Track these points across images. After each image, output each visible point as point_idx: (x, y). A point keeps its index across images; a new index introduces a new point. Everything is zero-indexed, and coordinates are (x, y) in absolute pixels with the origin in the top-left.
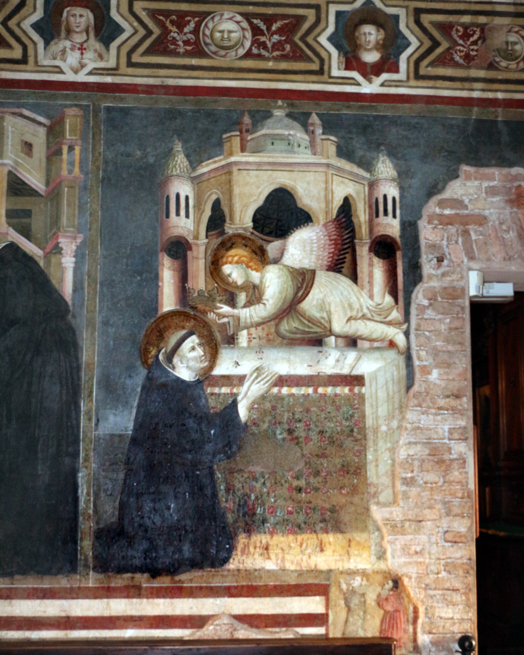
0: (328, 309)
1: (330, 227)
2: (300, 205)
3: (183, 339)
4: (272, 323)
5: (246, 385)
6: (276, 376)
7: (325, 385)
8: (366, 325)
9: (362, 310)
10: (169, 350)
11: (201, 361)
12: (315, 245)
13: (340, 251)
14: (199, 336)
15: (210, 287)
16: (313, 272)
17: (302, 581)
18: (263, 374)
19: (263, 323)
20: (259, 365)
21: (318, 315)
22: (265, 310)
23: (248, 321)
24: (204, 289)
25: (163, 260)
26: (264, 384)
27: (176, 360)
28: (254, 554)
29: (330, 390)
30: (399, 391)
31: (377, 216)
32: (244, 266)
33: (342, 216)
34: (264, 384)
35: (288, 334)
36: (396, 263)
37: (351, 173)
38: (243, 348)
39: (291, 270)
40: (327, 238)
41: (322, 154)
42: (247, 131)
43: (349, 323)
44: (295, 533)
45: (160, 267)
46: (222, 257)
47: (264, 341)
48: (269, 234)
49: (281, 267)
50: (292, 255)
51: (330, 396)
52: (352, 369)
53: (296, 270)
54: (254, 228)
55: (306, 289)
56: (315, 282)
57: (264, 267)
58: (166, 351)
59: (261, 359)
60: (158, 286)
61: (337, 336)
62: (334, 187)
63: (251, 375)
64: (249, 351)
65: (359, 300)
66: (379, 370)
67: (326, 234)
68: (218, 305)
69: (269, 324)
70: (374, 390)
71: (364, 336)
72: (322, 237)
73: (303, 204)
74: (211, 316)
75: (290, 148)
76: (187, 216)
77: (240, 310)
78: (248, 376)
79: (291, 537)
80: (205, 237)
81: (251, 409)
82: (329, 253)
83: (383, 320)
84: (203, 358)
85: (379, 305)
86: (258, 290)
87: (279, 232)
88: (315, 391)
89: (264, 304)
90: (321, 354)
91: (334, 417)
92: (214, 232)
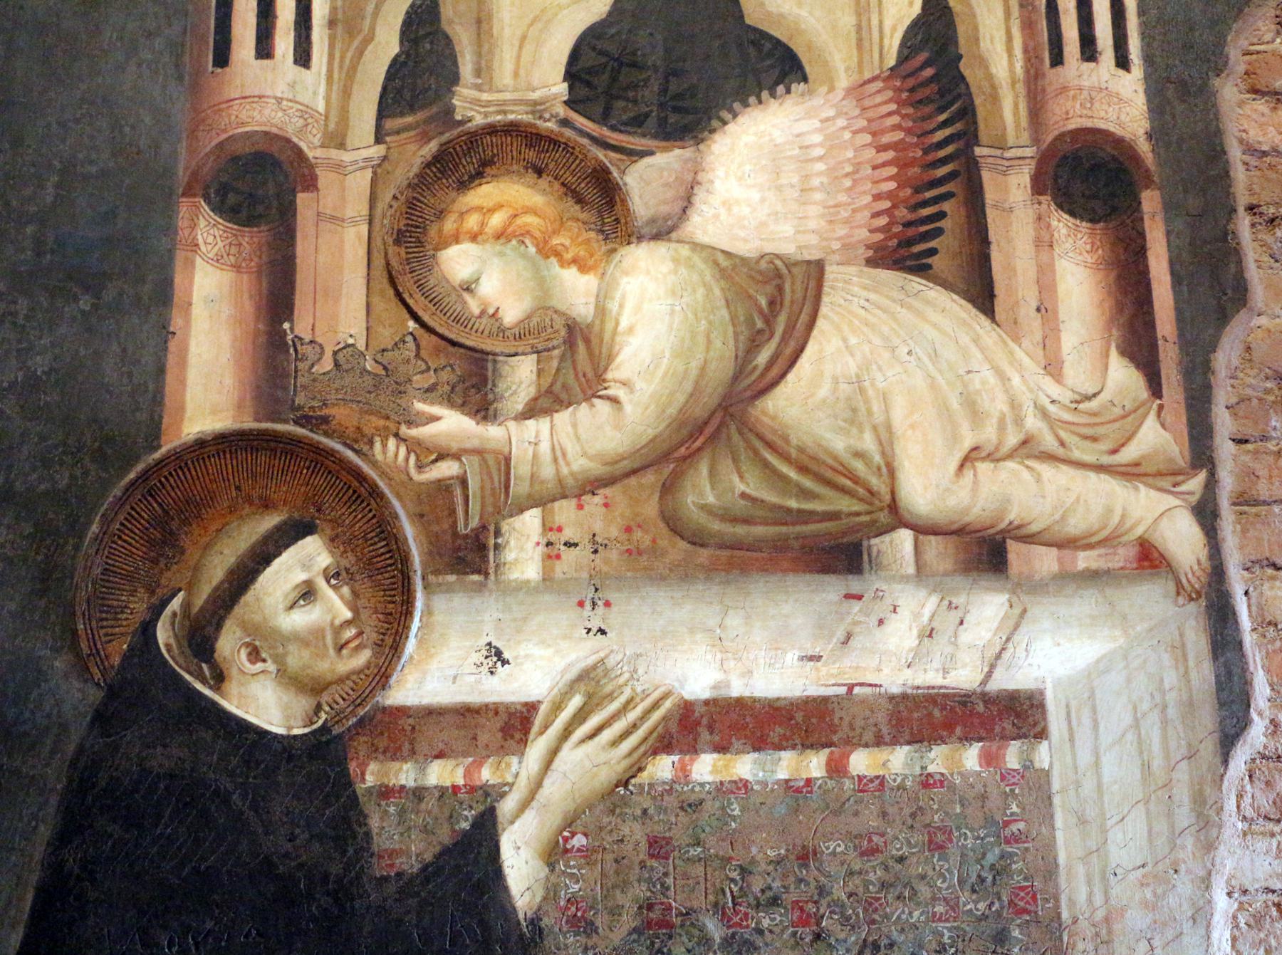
0: (879, 417)
1: (879, 99)
3: (262, 556)
4: (650, 478)
5: (537, 749)
6: (668, 704)
7: (879, 742)
8: (1038, 479)
9: (1019, 421)
10: (199, 602)
11: (340, 648)
12: (820, 167)
13: (917, 191)
15: (386, 336)
16: (817, 270)
18: (610, 697)
19: (609, 481)
20: (591, 661)
21: (839, 444)
22: (617, 427)
23: (547, 472)
24: (361, 345)
25: (193, 226)
26: (615, 743)
27: (229, 643)
31: (1057, 59)
32: (532, 250)
33: (923, 56)
34: (615, 743)
35: (716, 526)
36: (1142, 235)
38: (522, 587)
39: (724, 262)
40: (868, 138)
43: (968, 473)
45: (180, 256)
46: (441, 214)
47: (614, 555)
48: (636, 123)
49: (685, 251)
50: (727, 204)
52: (992, 667)
53: (744, 261)
55: (784, 340)
56: (824, 310)
57: (614, 251)
58: (186, 605)
59: (602, 631)
60: (164, 332)
61: (923, 530)
63: (557, 707)
64: (548, 598)
65: (1003, 378)
66: (1100, 668)
68: (420, 406)
69: (633, 481)
70: (1085, 757)
71: (1034, 528)
72: (847, 135)
73: (769, 14)
74: (390, 452)
76: (303, 57)
77: (512, 425)
78: (543, 709)
81: (554, 853)
82: (877, 197)
83: (1106, 460)
84: (350, 633)
85: (1089, 398)
86: (587, 341)
87: (673, 119)
88: (837, 768)
89: (614, 400)
90: (856, 606)
91: (923, 877)
92: (409, 119)
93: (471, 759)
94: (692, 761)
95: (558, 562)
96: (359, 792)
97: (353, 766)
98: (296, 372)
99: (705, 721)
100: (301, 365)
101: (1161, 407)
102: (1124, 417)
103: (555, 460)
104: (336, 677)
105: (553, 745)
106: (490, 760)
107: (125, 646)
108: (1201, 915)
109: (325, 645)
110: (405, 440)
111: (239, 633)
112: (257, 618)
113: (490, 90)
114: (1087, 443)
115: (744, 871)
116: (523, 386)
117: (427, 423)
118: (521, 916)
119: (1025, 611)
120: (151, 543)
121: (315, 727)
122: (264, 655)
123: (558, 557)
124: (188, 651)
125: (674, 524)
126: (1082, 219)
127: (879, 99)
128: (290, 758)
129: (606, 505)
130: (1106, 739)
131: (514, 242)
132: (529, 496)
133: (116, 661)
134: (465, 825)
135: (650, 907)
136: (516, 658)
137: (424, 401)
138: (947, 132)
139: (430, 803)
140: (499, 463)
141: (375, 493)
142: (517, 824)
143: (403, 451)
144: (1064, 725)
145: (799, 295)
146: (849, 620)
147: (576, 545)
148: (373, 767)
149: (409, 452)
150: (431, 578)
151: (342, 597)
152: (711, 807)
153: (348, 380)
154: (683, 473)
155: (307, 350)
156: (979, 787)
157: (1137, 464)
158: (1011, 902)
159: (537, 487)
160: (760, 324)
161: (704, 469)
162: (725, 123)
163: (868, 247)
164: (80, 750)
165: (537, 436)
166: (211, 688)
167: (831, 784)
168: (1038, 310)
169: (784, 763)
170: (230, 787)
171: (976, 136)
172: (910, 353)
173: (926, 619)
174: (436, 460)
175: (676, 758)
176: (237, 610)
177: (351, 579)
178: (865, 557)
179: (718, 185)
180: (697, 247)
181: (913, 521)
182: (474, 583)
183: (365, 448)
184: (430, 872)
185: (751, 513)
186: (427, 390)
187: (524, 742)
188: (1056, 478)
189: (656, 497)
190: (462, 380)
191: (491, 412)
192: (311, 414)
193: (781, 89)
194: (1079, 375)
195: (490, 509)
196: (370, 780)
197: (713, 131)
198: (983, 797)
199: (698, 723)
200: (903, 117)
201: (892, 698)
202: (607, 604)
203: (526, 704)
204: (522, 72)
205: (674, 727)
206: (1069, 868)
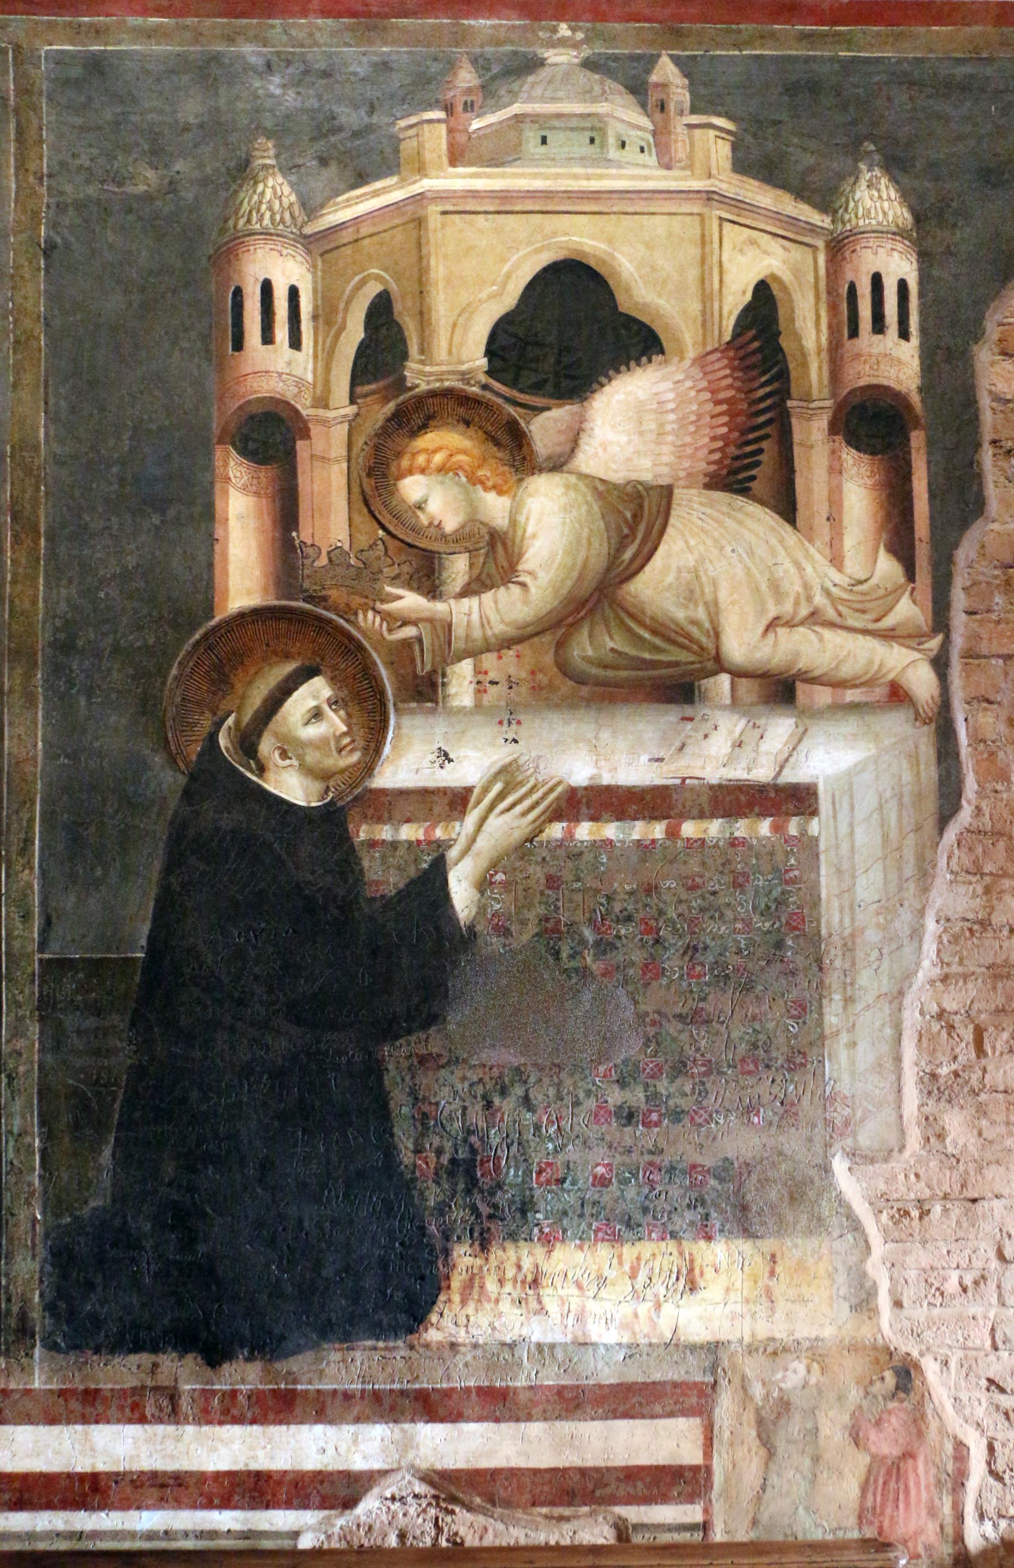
0: (709, 596)
1: (717, 366)
2: (624, 305)
4: (547, 638)
5: (472, 818)
6: (560, 789)
7: (702, 816)
8: (821, 640)
9: (809, 599)
11: (340, 751)
12: (672, 417)
13: (743, 433)
14: (332, 680)
16: (667, 493)
17: (634, 1375)
18: (521, 784)
19: (519, 640)
20: (507, 760)
21: (680, 615)
22: (525, 603)
23: (477, 633)
24: (346, 547)
26: (524, 814)
27: (267, 746)
28: (497, 1301)
29: (714, 828)
30: (918, 829)
31: (854, 333)
32: (464, 479)
34: (524, 814)
35: (594, 671)
36: (909, 464)
37: (778, 217)
38: (462, 710)
40: (707, 395)
41: (690, 167)
42: (469, 107)
43: (771, 636)
44: (616, 1239)
46: (399, 455)
47: (524, 690)
48: (537, 388)
49: (573, 479)
50: (604, 446)
51: (716, 846)
52: (782, 767)
53: (616, 486)
54: (490, 373)
55: (643, 542)
56: (672, 520)
57: (521, 480)
58: (237, 722)
59: (515, 741)
60: (211, 540)
61: (738, 674)
62: (725, 257)
63: (486, 790)
65: (800, 568)
67: (704, 384)
68: (389, 589)
69: (536, 639)
70: (844, 829)
72: (693, 393)
73: (637, 304)
75: (593, 150)
77: (452, 602)
78: (476, 792)
79: (604, 1251)
80: (347, 402)
81: (483, 885)
82: (714, 439)
83: (872, 626)
84: (346, 740)
85: (860, 582)
86: (504, 544)
87: (565, 383)
88: (673, 833)
89: (523, 585)
90: (689, 726)
91: (728, 905)
92: (373, 386)
94: (575, 827)
97: (351, 826)
99: (584, 800)
100: (305, 561)
101: (913, 589)
102: (886, 596)
103: (483, 625)
108: (917, 933)
111: (273, 740)
112: (284, 730)
113: (431, 365)
114: (857, 614)
115: (609, 898)
118: (462, 923)
119: (806, 730)
120: (213, 682)
123: (485, 691)
124: (240, 752)
125: (564, 668)
126: (865, 452)
127: (717, 366)
129: (518, 656)
130: (860, 815)
131: (451, 474)
134: (425, 866)
135: (547, 920)
137: (391, 585)
138: (768, 389)
139: (401, 851)
141: (360, 648)
142: (460, 865)
143: (378, 619)
144: (830, 807)
145: (654, 510)
146: (683, 735)
147: (497, 683)
150: (400, 705)
152: (588, 857)
153: (338, 570)
154: (571, 634)
155: (310, 551)
156: (769, 848)
157: (893, 630)
158: (787, 923)
159: (470, 644)
160: (626, 531)
161: (585, 631)
162: (602, 386)
163: (705, 475)
164: (176, 813)
167: (668, 843)
168: (828, 519)
169: (637, 829)
170: (272, 839)
171: (789, 393)
172: (733, 551)
173: (737, 734)
174: (401, 626)
175: (565, 824)
176: (272, 726)
178: (697, 693)
179: (597, 431)
180: (582, 476)
181: (732, 668)
183: (352, 618)
184: (402, 895)
185: (618, 660)
186: (394, 578)
187: (463, 813)
188: (833, 638)
189: (552, 651)
193: (644, 359)
194: (855, 565)
196: (363, 836)
197: (594, 392)
198: (772, 854)
199: (579, 802)
200: (735, 379)
201: (711, 787)
202: (519, 723)
204: (454, 350)
205: (564, 804)
206: (828, 902)
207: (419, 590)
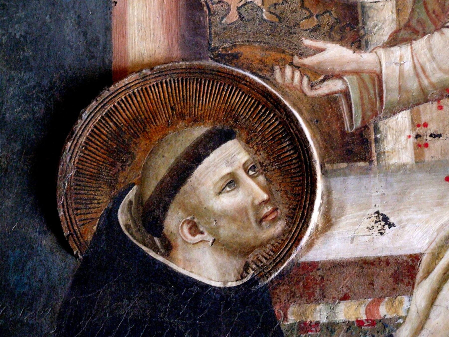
11: (260, 221)
23: (413, 85)
58: (139, 196)
64: (420, 176)
68: (307, 42)
77: (381, 52)
78: (425, 259)
84: (267, 209)
93: (370, 300)
95: (426, 149)
96: (282, 328)
97: (277, 309)
98: (210, 23)
100: (213, 19)
103: (417, 75)
104: (258, 242)
105: (435, 285)
106: (386, 299)
107: (95, 228)
109: (248, 219)
110: (298, 67)
111: (181, 214)
112: (194, 201)
116: (387, 23)
117: (314, 54)
120: (110, 151)
121: (245, 280)
122: (201, 229)
123: (426, 145)
124: (143, 229)
128: (228, 304)
132: (399, 102)
133: (89, 238)
136: (400, 222)
137: (311, 38)
140: (373, 80)
141: (277, 104)
143: (297, 74)
147: (440, 136)
148: (292, 309)
149: (302, 76)
150: (327, 166)
151: (258, 184)
159: (404, 96)
164: (66, 304)
165: (401, 59)
166: (162, 255)
170: (182, 328)
174: (324, 80)
176: (179, 197)
177: (265, 170)
182: (361, 168)
183: (268, 75)
190: (338, 21)
191: (363, 43)
192: (224, 52)
195: (369, 113)
196: (291, 319)
203: (411, 256)
207: (342, 41)
